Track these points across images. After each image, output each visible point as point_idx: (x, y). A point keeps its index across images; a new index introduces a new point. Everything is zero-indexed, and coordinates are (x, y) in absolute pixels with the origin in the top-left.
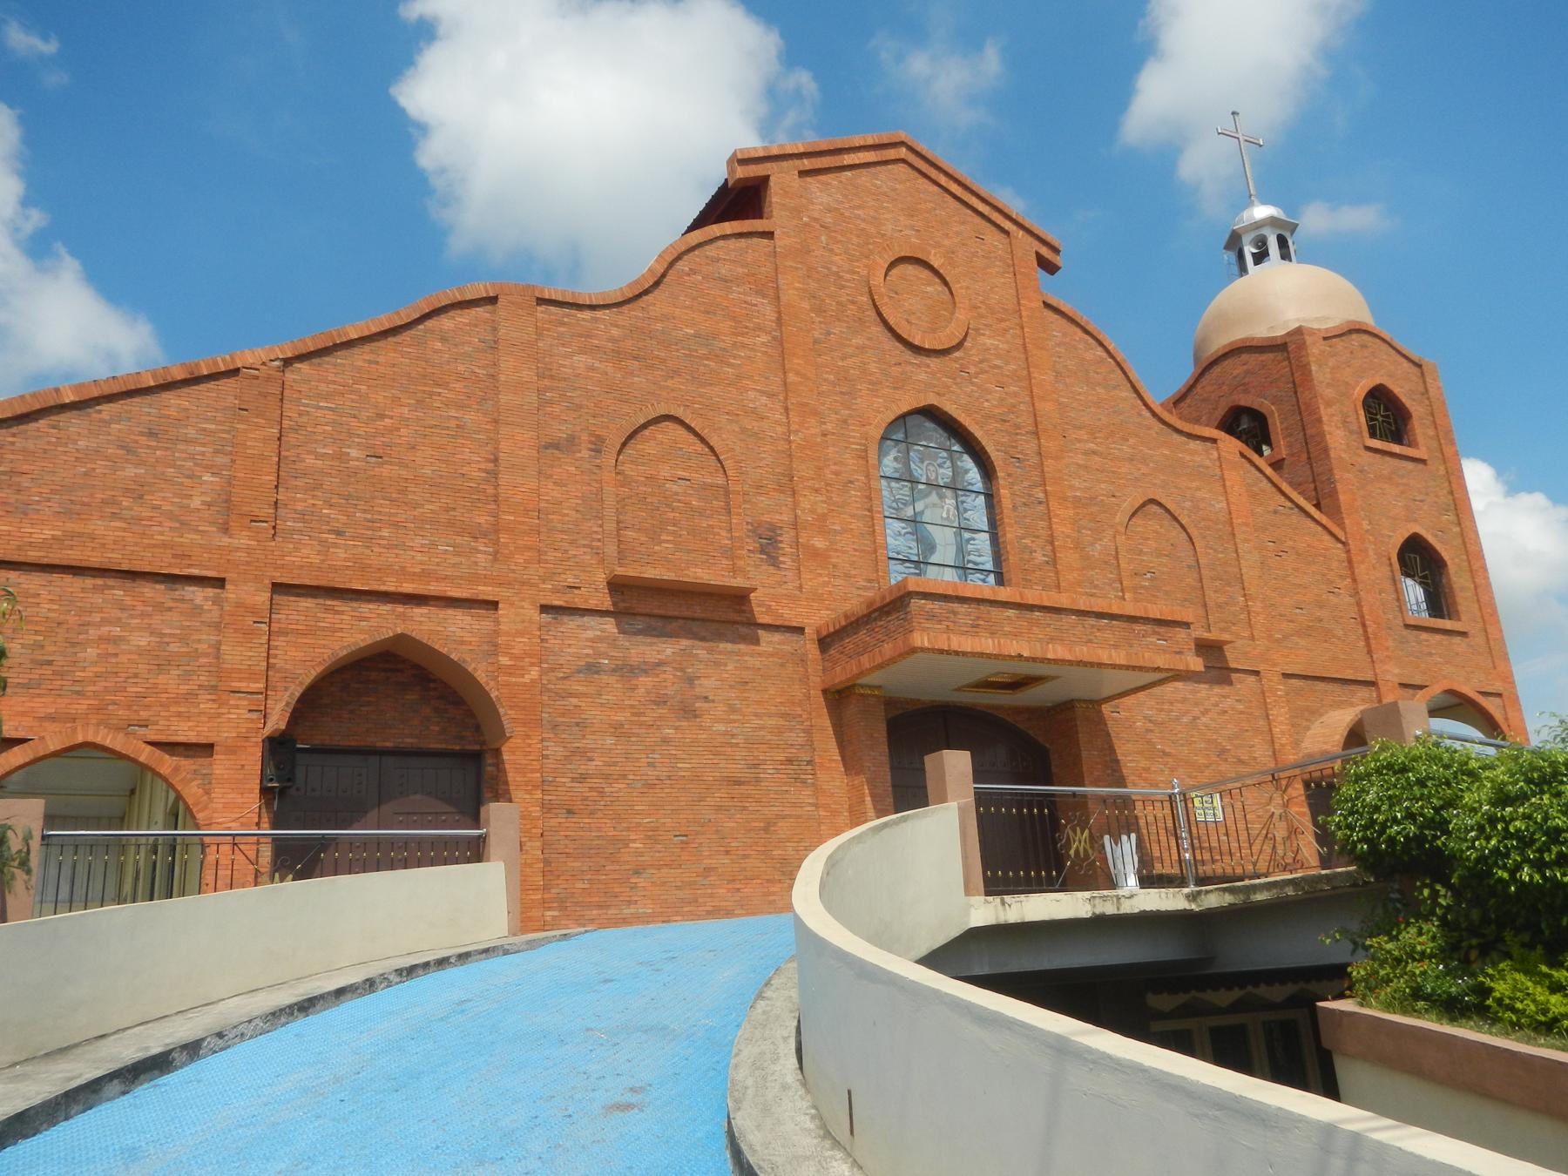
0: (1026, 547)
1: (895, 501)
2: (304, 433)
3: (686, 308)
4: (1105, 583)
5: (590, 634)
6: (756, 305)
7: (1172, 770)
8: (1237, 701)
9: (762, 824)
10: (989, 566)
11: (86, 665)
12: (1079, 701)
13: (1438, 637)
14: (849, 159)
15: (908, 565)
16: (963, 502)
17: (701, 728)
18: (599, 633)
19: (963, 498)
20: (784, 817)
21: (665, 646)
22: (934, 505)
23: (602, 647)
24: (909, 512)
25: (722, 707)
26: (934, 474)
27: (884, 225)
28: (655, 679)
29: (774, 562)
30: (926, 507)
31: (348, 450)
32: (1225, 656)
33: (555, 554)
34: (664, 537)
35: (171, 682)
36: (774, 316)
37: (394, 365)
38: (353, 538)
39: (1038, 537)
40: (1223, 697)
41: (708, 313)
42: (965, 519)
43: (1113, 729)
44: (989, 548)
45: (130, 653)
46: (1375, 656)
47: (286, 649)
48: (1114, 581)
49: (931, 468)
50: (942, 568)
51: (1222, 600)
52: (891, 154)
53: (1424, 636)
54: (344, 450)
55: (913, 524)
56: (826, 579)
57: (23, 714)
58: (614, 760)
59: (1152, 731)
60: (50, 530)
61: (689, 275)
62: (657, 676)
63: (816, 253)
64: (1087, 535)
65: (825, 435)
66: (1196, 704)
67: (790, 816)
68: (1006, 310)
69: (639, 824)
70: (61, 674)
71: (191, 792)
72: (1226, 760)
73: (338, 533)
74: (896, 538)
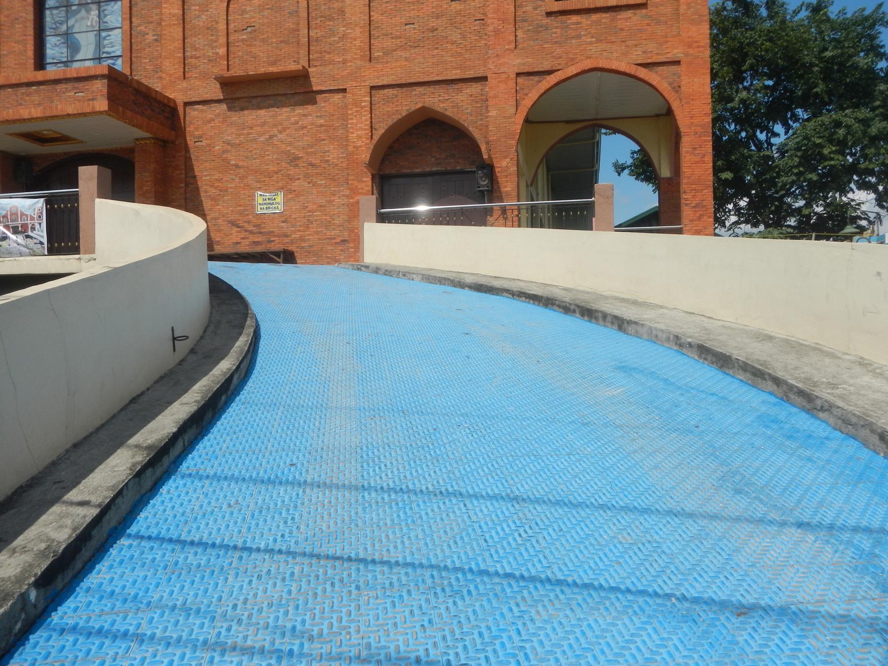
1: (55, 23)
4: (204, 45)
7: (242, 178)
12: (137, 139)
13: (595, 17)
15: (59, 65)
16: (104, 11)
22: (83, 18)
24: (64, 28)
30: (76, 21)
32: (310, 82)
39: (151, 22)
40: (304, 115)
43: (193, 154)
46: (490, 52)
48: (216, 41)
50: (83, 62)
51: (319, 35)
53: (574, 18)
64: (195, 10)
66: (275, 125)
72: (297, 165)
74: (54, 49)
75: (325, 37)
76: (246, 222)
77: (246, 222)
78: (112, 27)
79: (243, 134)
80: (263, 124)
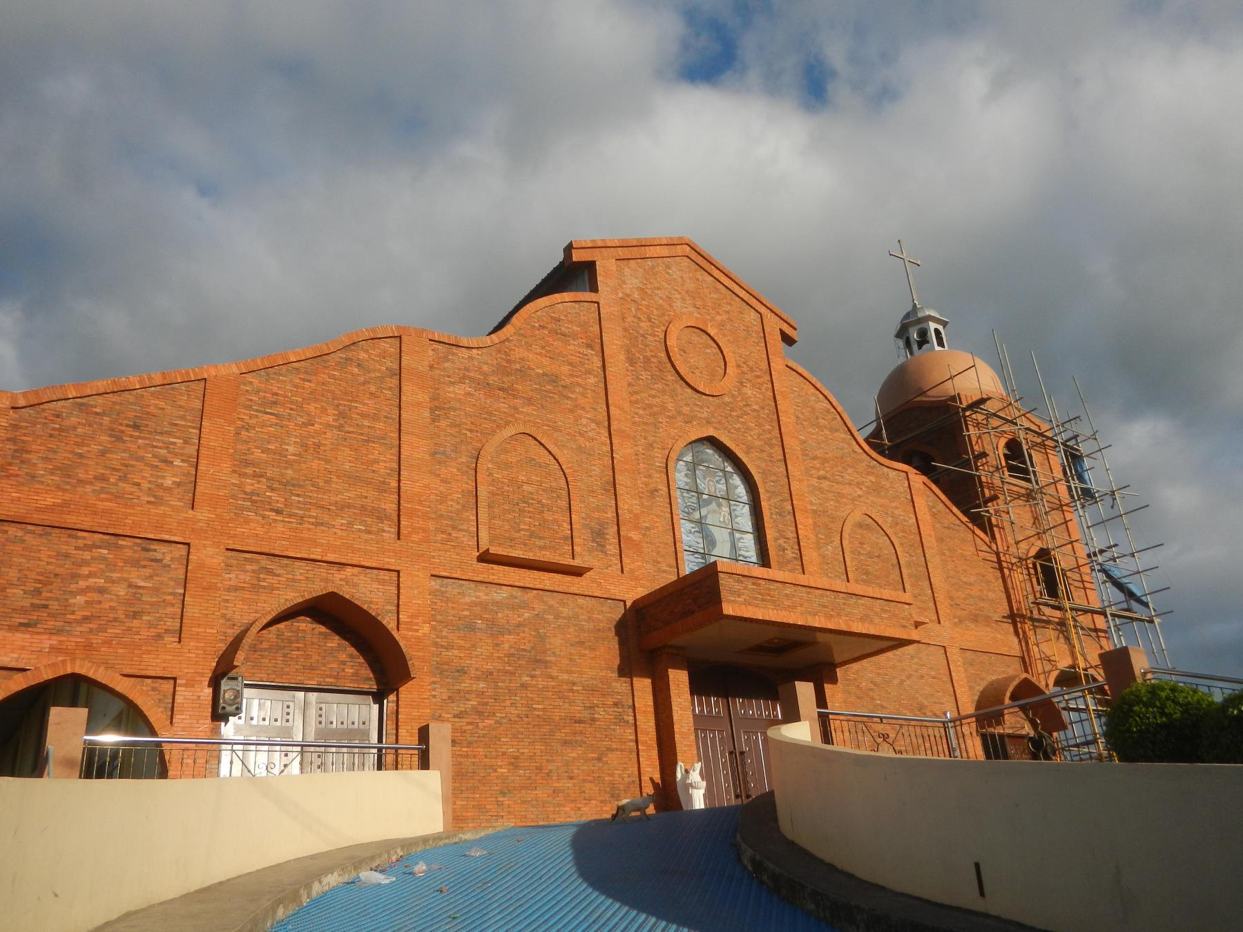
0: (780, 546)
2: (254, 432)
3: (537, 354)
5: (467, 599)
6: (587, 355)
9: (596, 756)
10: (754, 559)
11: (75, 609)
14: (650, 252)
16: (734, 510)
18: (474, 599)
19: (734, 507)
20: (613, 750)
21: (523, 611)
22: (714, 511)
23: (477, 609)
24: (696, 516)
25: (565, 661)
26: (713, 488)
27: (676, 302)
28: (516, 637)
29: (602, 547)
31: (287, 447)
33: (441, 535)
34: (522, 526)
35: (142, 626)
36: (600, 364)
37: (323, 384)
38: (290, 516)
41: (553, 358)
42: (737, 523)
44: (753, 546)
45: (111, 600)
47: (235, 602)
49: (711, 483)
52: (679, 250)
54: (283, 446)
56: (640, 564)
57: (23, 648)
58: (485, 700)
59: (873, 689)
60: (52, 498)
61: (539, 330)
62: (518, 634)
63: (629, 319)
64: (822, 539)
65: (637, 455)
67: (617, 749)
68: (761, 370)
69: (504, 754)
70: (53, 616)
71: (155, 715)
73: (278, 512)
74: (688, 535)
75: (920, 595)
79: (879, 674)
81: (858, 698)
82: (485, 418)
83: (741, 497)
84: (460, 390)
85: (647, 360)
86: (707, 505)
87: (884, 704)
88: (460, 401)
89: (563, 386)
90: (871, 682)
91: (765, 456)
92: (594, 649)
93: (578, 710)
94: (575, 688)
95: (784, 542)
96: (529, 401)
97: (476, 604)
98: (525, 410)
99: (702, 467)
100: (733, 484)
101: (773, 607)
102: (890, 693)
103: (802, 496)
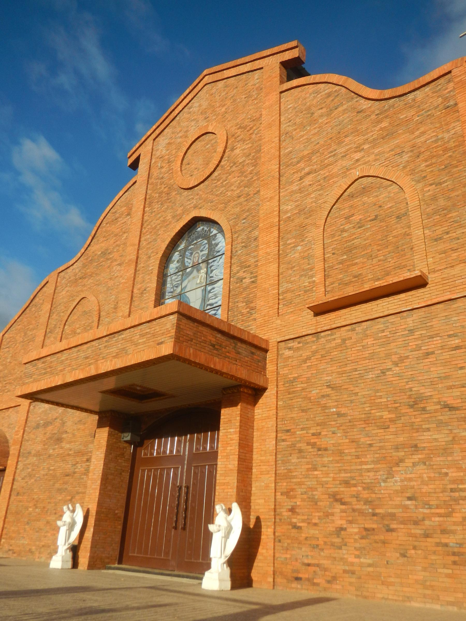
0: (238, 278)
5: (41, 410)
6: (125, 222)
8: (449, 336)
12: (225, 389)
14: (177, 111)
16: (211, 267)
17: (62, 448)
22: (194, 278)
24: (179, 290)
30: (189, 282)
41: (107, 239)
51: (439, 232)
55: (179, 296)
59: (328, 396)
64: (290, 244)
66: (388, 356)
72: (424, 409)
75: (447, 233)
76: (353, 496)
77: (353, 496)
78: (216, 280)
79: (344, 372)
80: (372, 357)
81: (303, 411)
82: (71, 301)
83: (219, 252)
84: (64, 292)
85: (161, 193)
86: (188, 277)
87: (343, 410)
88: (63, 298)
89: (109, 253)
90: (328, 386)
91: (242, 199)
92: (85, 424)
93: (68, 467)
94: (70, 453)
95: (244, 272)
96: (91, 276)
97: (43, 412)
98: (88, 283)
99: (192, 246)
100: (215, 244)
101: (50, 376)
102: (356, 394)
103: (270, 214)
